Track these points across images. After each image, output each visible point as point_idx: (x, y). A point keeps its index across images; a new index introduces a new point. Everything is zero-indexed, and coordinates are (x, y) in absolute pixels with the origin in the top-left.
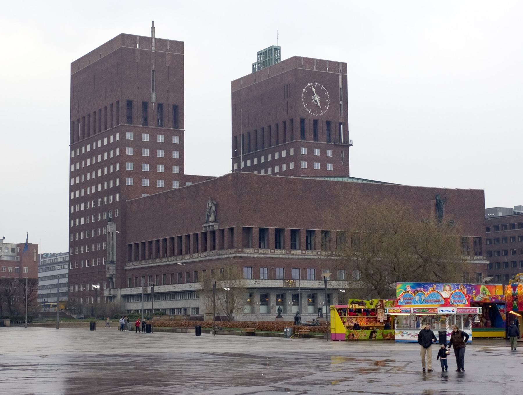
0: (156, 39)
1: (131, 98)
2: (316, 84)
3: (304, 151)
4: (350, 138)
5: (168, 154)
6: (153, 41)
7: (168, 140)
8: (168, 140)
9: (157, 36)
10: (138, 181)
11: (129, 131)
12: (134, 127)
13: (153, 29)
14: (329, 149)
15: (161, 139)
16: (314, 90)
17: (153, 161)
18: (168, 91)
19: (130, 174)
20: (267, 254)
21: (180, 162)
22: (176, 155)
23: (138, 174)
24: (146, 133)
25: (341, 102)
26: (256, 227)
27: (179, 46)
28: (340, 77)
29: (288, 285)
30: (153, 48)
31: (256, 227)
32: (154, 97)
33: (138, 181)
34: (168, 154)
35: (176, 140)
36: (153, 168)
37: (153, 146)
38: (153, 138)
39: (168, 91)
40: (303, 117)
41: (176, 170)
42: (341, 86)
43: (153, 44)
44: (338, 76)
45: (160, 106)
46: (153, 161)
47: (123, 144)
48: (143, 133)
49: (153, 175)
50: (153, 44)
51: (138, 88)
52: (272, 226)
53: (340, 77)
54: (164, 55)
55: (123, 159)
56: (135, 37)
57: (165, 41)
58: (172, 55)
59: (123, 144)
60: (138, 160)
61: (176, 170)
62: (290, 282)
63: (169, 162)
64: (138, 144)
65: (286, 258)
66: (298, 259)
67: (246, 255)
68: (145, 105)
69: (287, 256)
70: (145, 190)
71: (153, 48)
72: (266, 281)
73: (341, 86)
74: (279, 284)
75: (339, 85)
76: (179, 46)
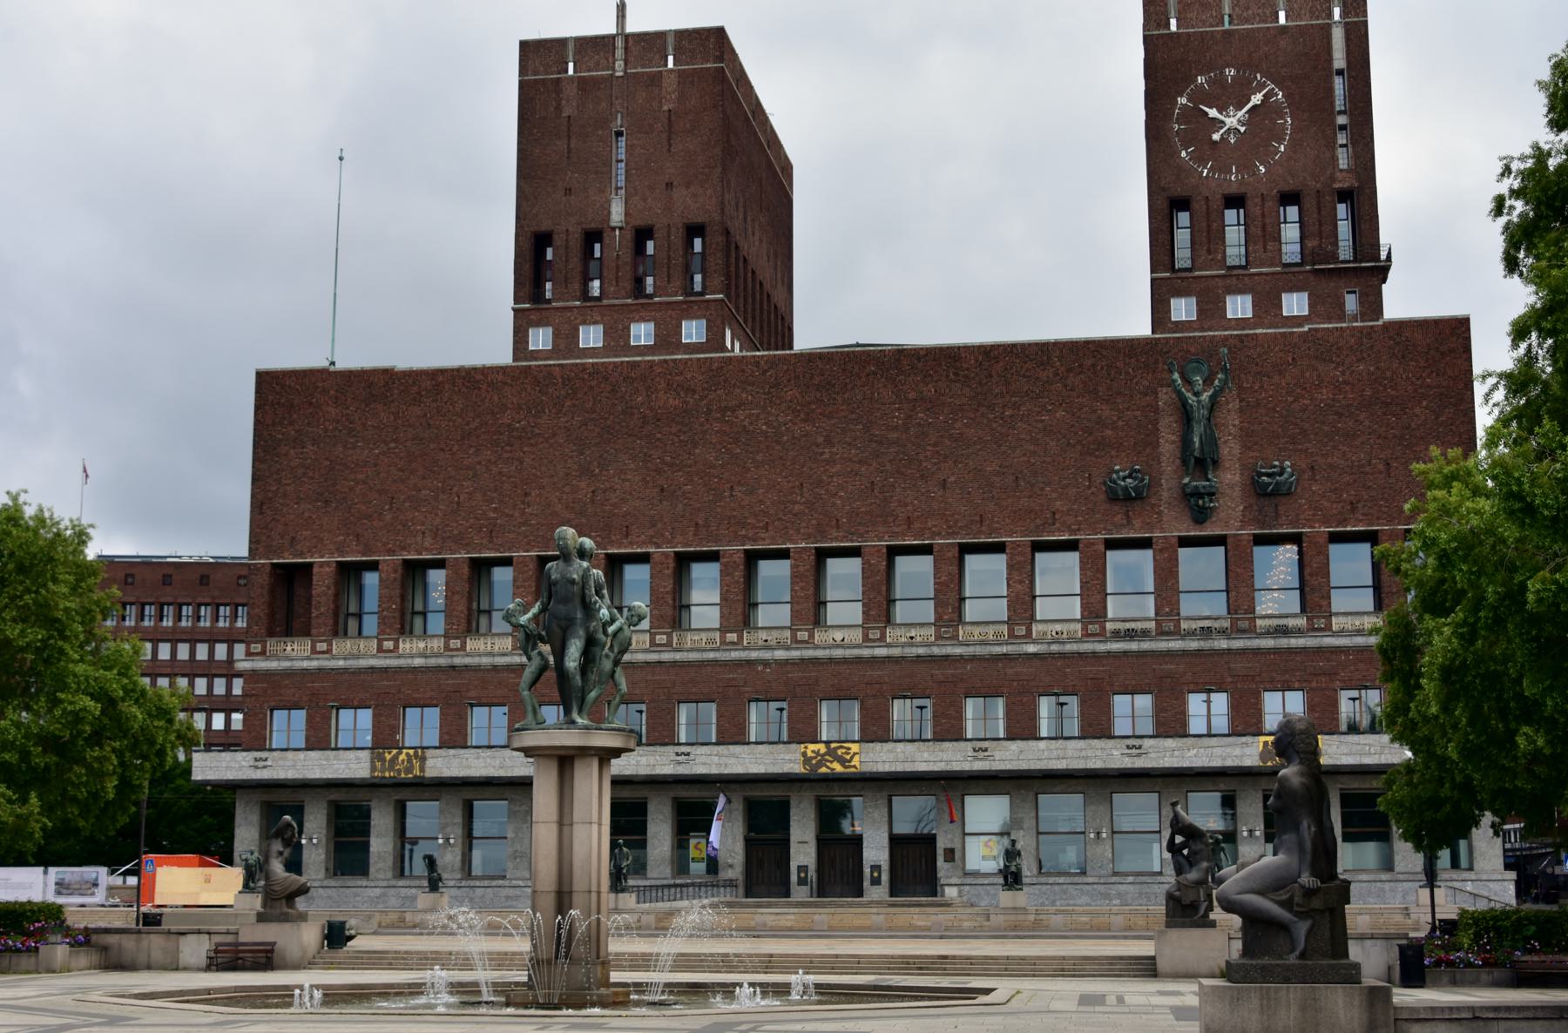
0: (627, 37)
1: (545, 226)
2: (1230, 72)
4: (1384, 238)
6: (620, 43)
9: (632, 27)
11: (538, 324)
12: (557, 309)
13: (621, 9)
14: (1291, 290)
16: (1256, 99)
18: (669, 185)
20: (364, 656)
24: (595, 323)
25: (1342, 120)
26: (323, 561)
28: (1338, 36)
29: (391, 769)
30: (619, 65)
31: (323, 561)
32: (617, 214)
39: (669, 185)
40: (1178, 191)
42: (1339, 60)
43: (619, 53)
44: (1326, 30)
45: (642, 235)
48: (584, 323)
50: (619, 53)
51: (568, 191)
52: (391, 552)
53: (1338, 36)
54: (655, 79)
56: (561, 43)
57: (660, 36)
58: (681, 74)
62: (402, 757)
65: (438, 668)
66: (495, 668)
67: (273, 665)
69: (442, 661)
71: (619, 65)
72: (301, 755)
73: (1339, 60)
74: (354, 766)
75: (1330, 60)
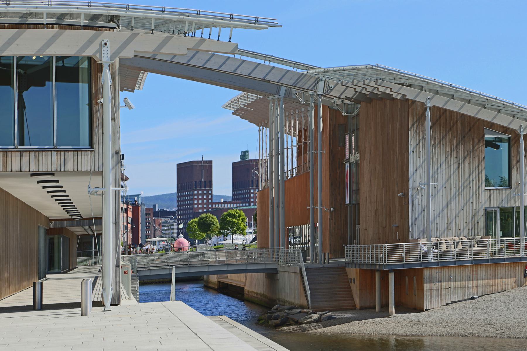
3: (252, 191)
5: (208, 197)
7: (207, 192)
8: (207, 192)
10: (198, 206)
15: (205, 192)
17: (203, 199)
19: (196, 204)
21: (211, 199)
22: (210, 197)
23: (198, 204)
27: (211, 162)
33: (198, 206)
34: (208, 197)
35: (210, 192)
36: (203, 201)
37: (203, 194)
38: (203, 192)
41: (210, 201)
45: (205, 182)
46: (203, 199)
47: (193, 195)
49: (203, 204)
55: (193, 199)
59: (193, 195)
60: (198, 199)
61: (210, 201)
63: (208, 199)
64: (198, 195)
68: (201, 181)
70: (200, 208)
76: (211, 162)
